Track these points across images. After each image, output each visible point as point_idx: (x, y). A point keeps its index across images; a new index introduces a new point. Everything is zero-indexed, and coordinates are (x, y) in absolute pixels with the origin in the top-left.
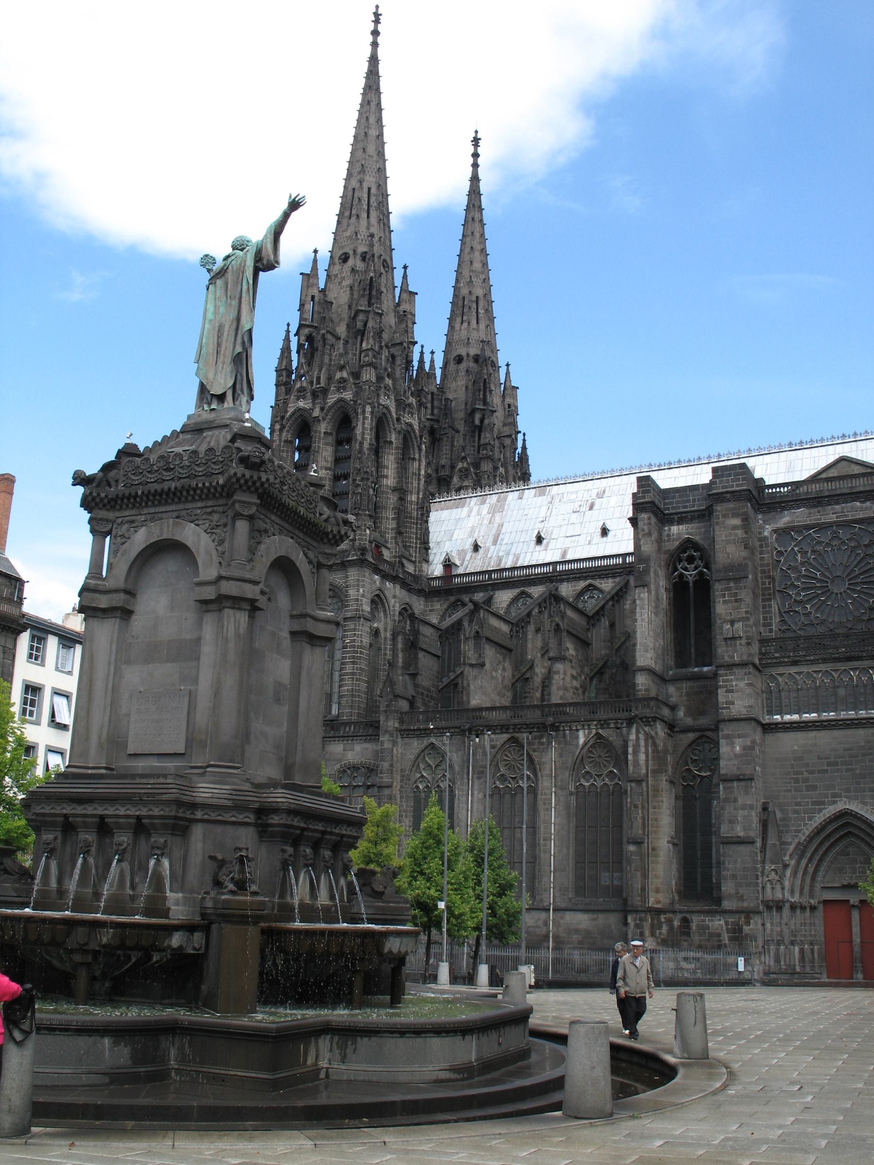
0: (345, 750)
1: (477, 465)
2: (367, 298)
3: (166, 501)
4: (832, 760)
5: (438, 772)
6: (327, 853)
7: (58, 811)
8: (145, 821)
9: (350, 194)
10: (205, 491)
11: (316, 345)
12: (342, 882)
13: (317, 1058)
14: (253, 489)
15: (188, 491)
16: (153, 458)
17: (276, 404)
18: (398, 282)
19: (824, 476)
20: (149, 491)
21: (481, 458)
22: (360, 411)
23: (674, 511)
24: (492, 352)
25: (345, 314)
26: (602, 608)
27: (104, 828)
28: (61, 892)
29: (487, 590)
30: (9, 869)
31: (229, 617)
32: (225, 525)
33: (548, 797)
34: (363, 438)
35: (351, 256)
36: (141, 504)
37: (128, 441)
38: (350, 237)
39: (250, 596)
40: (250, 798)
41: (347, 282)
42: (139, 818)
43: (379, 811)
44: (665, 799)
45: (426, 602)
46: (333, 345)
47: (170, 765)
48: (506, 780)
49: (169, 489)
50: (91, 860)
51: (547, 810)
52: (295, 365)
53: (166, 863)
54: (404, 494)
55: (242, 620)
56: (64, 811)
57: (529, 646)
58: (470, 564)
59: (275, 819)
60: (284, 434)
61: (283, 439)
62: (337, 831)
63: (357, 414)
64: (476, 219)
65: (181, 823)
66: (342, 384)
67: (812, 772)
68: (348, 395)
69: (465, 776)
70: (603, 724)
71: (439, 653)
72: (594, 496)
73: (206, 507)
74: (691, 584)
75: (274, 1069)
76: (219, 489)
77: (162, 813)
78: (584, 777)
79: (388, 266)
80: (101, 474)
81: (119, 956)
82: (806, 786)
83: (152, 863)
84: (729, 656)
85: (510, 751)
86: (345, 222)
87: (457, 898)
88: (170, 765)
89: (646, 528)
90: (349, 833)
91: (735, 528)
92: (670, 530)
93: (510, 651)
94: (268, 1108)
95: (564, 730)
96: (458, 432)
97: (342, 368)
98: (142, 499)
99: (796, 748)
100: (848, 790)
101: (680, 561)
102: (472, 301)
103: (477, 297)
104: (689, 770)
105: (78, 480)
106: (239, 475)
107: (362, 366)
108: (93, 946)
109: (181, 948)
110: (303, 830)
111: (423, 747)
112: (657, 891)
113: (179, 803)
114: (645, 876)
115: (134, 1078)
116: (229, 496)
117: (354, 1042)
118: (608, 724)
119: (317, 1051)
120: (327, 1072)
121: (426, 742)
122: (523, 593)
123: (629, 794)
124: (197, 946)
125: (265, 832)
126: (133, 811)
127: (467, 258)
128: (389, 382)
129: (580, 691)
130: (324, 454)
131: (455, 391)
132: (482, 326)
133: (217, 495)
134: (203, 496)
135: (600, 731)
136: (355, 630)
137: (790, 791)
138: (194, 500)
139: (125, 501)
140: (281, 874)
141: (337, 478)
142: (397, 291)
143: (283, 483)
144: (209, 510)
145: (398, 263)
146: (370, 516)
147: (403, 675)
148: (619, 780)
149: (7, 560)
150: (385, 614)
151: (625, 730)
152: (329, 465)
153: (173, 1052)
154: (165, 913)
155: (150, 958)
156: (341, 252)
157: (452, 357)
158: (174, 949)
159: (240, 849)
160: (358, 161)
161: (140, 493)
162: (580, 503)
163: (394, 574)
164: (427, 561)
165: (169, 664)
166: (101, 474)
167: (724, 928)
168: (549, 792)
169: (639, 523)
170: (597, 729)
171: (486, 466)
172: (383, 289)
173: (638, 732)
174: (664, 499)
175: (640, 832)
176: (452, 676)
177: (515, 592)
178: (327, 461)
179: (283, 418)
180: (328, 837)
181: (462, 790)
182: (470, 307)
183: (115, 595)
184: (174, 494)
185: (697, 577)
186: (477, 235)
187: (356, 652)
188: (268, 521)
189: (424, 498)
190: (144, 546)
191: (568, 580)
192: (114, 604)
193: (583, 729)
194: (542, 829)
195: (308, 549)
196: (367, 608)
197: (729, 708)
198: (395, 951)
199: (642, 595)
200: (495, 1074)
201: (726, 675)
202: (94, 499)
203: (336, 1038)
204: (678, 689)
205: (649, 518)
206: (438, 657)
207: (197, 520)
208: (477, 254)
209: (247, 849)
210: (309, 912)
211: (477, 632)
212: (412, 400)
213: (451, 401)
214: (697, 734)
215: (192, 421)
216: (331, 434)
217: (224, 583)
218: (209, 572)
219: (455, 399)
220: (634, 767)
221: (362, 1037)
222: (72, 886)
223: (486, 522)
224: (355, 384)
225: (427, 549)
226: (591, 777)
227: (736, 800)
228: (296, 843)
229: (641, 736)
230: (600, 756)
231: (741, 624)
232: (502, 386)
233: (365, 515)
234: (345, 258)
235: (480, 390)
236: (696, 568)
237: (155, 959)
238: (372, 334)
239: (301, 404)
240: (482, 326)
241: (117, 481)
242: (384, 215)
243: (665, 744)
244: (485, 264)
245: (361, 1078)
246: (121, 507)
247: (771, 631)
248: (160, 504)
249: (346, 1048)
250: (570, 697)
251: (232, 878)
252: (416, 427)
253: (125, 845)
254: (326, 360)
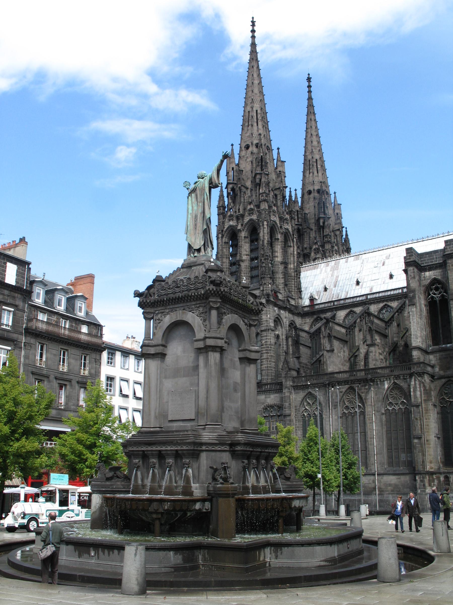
0: (265, 398)
1: (323, 246)
2: (260, 167)
3: (178, 302)
5: (314, 406)
6: (263, 462)
7: (140, 449)
8: (180, 452)
9: (247, 114)
10: (195, 297)
11: (236, 193)
12: (271, 474)
13: (264, 557)
14: (217, 295)
15: (187, 297)
16: (170, 282)
17: (218, 224)
18: (275, 156)
20: (170, 298)
21: (325, 243)
22: (261, 224)
23: (426, 265)
24: (326, 187)
25: (250, 175)
26: (393, 317)
27: (161, 456)
28: (144, 486)
29: (333, 311)
30: (119, 476)
31: (211, 355)
32: (206, 312)
33: (371, 416)
34: (264, 238)
35: (250, 146)
36: (166, 304)
37: (157, 274)
38: (249, 137)
39: (220, 345)
40: (227, 439)
41: (249, 160)
42: (177, 451)
43: (285, 430)
44: (431, 415)
45: (302, 319)
46: (245, 192)
47: (188, 425)
48: (349, 408)
49: (179, 297)
50: (156, 471)
51: (371, 423)
52: (226, 203)
53: (190, 471)
54: (287, 265)
55: (217, 356)
56: (143, 449)
57: (356, 338)
58: (323, 298)
59: (239, 448)
60: (224, 239)
61: (224, 241)
62: (267, 451)
63: (260, 226)
64: (312, 119)
65: (196, 452)
66: (251, 212)
68: (254, 217)
69: (328, 408)
70: (397, 377)
71: (310, 345)
72: (384, 258)
73: (196, 304)
74: (438, 302)
75: (246, 563)
76: (202, 296)
77: (187, 448)
78: (389, 405)
79: (269, 149)
80: (147, 291)
81: (173, 514)
83: (184, 471)
85: (350, 394)
86: (246, 129)
87: (327, 472)
88: (189, 424)
89: (412, 274)
90: (272, 451)
92: (425, 274)
93: (346, 342)
94: (244, 581)
95: (377, 382)
96: (312, 230)
97: (250, 203)
98: (166, 302)
101: (431, 290)
102: (314, 162)
103: (316, 160)
104: (443, 398)
105: (137, 295)
106: (211, 289)
108: (161, 510)
109: (200, 509)
110: (252, 451)
111: (305, 394)
112: (431, 462)
113: (194, 444)
114: (424, 455)
115: (184, 569)
116: (207, 298)
117: (281, 550)
118: (400, 377)
119: (264, 554)
120: (269, 564)
121: (306, 392)
122: (351, 311)
123: (413, 412)
124: (207, 508)
125: (234, 454)
126: (174, 448)
127: (309, 140)
128: (275, 208)
129: (384, 361)
130: (245, 247)
131: (309, 209)
132: (320, 174)
133: (201, 298)
134: (195, 299)
135: (396, 381)
136: (267, 336)
138: (190, 301)
139: (159, 303)
140: (243, 473)
141: (252, 259)
142: (275, 161)
143: (231, 289)
144: (198, 306)
145: (274, 146)
146: (270, 278)
147: (293, 358)
148: (407, 406)
149: (93, 316)
150: (282, 327)
151: (408, 379)
152: (248, 253)
153: (200, 557)
154: (191, 494)
155: (186, 514)
156: (245, 144)
157: (306, 191)
158: (197, 510)
159: (224, 464)
160: (250, 97)
161: (165, 299)
162: (377, 262)
163: (285, 306)
164: (301, 298)
165: (185, 379)
166: (147, 291)
168: (371, 414)
169: (408, 272)
170: (394, 380)
171: (328, 246)
172: (268, 161)
173: (415, 380)
174: (421, 258)
175: (420, 432)
176: (318, 357)
177: (347, 311)
178: (247, 251)
179: (222, 231)
180: (263, 454)
181: (327, 415)
182: (313, 165)
183: (157, 348)
184: (181, 299)
185: (441, 298)
186: (314, 127)
187: (267, 347)
188: (225, 308)
189: (297, 266)
190: (169, 324)
191: (374, 303)
192: (157, 352)
193: (387, 380)
194: (369, 432)
195: (245, 318)
196: (272, 325)
198: (297, 506)
199: (413, 309)
200: (346, 563)
202: (144, 303)
203: (273, 548)
204: (434, 356)
205: (413, 269)
206: (310, 347)
207: (193, 310)
208: (314, 137)
209: (227, 463)
210: (256, 490)
211: (329, 334)
212: (288, 216)
213: (307, 214)
214: (447, 380)
215: (186, 262)
216: (247, 237)
217: (207, 340)
218: (200, 335)
219: (309, 213)
220: (414, 398)
221: (284, 547)
222: (148, 482)
223: (330, 275)
224: (257, 211)
225: (300, 292)
226: (393, 405)
228: (248, 458)
229: (417, 382)
230: (396, 394)
232: (333, 204)
233: (268, 277)
234: (247, 147)
235: (321, 207)
236: (440, 293)
237: (188, 515)
238: (264, 185)
239: (231, 223)
240: (320, 174)
241: (154, 294)
242: (265, 123)
243: (430, 386)
244: (319, 142)
245: (284, 566)
246: (157, 306)
248: (175, 304)
249: (277, 552)
250: (379, 364)
251: (221, 477)
252: (290, 230)
253: (171, 463)
254: (242, 200)
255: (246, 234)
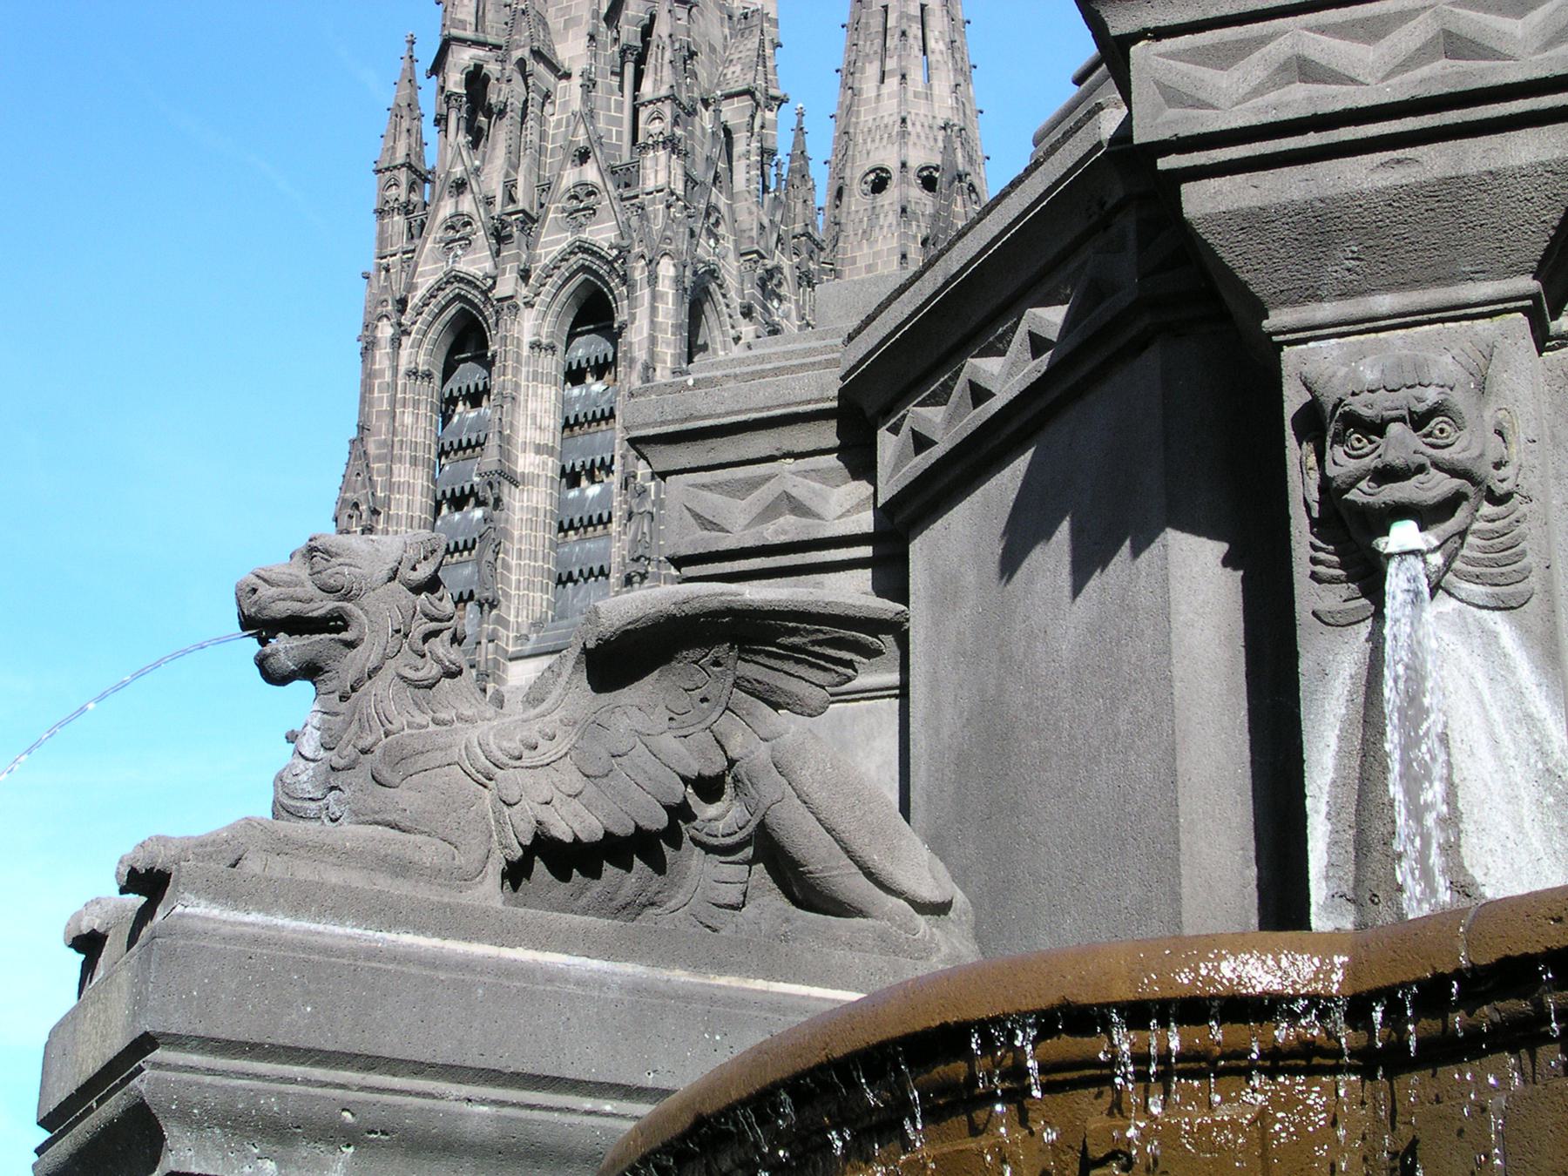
34: (652, 354)
60: (405, 353)
61: (402, 369)
68: (602, 234)
102: (910, 18)
103: (923, 7)
107: (646, 147)
157: (859, 174)
179: (402, 303)
238: (668, 55)
255: (545, 331)
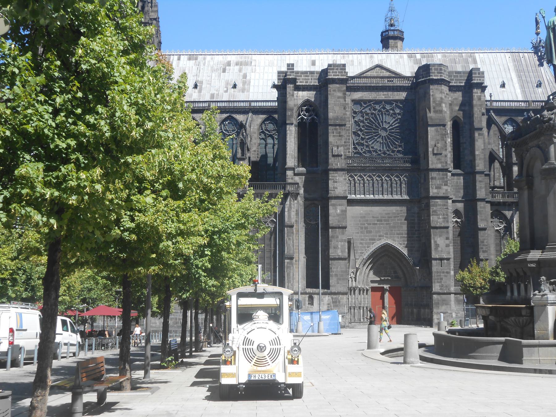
4: (380, 218)
19: (369, 74)
67: (370, 224)
74: (308, 124)
82: (367, 231)
84: (335, 164)
91: (339, 97)
92: (298, 94)
99: (362, 212)
100: (387, 234)
101: (302, 111)
137: (358, 233)
167: (331, 300)
197: (334, 190)
201: (333, 174)
227: (337, 237)
231: (342, 148)
236: (310, 116)
247: (349, 152)
